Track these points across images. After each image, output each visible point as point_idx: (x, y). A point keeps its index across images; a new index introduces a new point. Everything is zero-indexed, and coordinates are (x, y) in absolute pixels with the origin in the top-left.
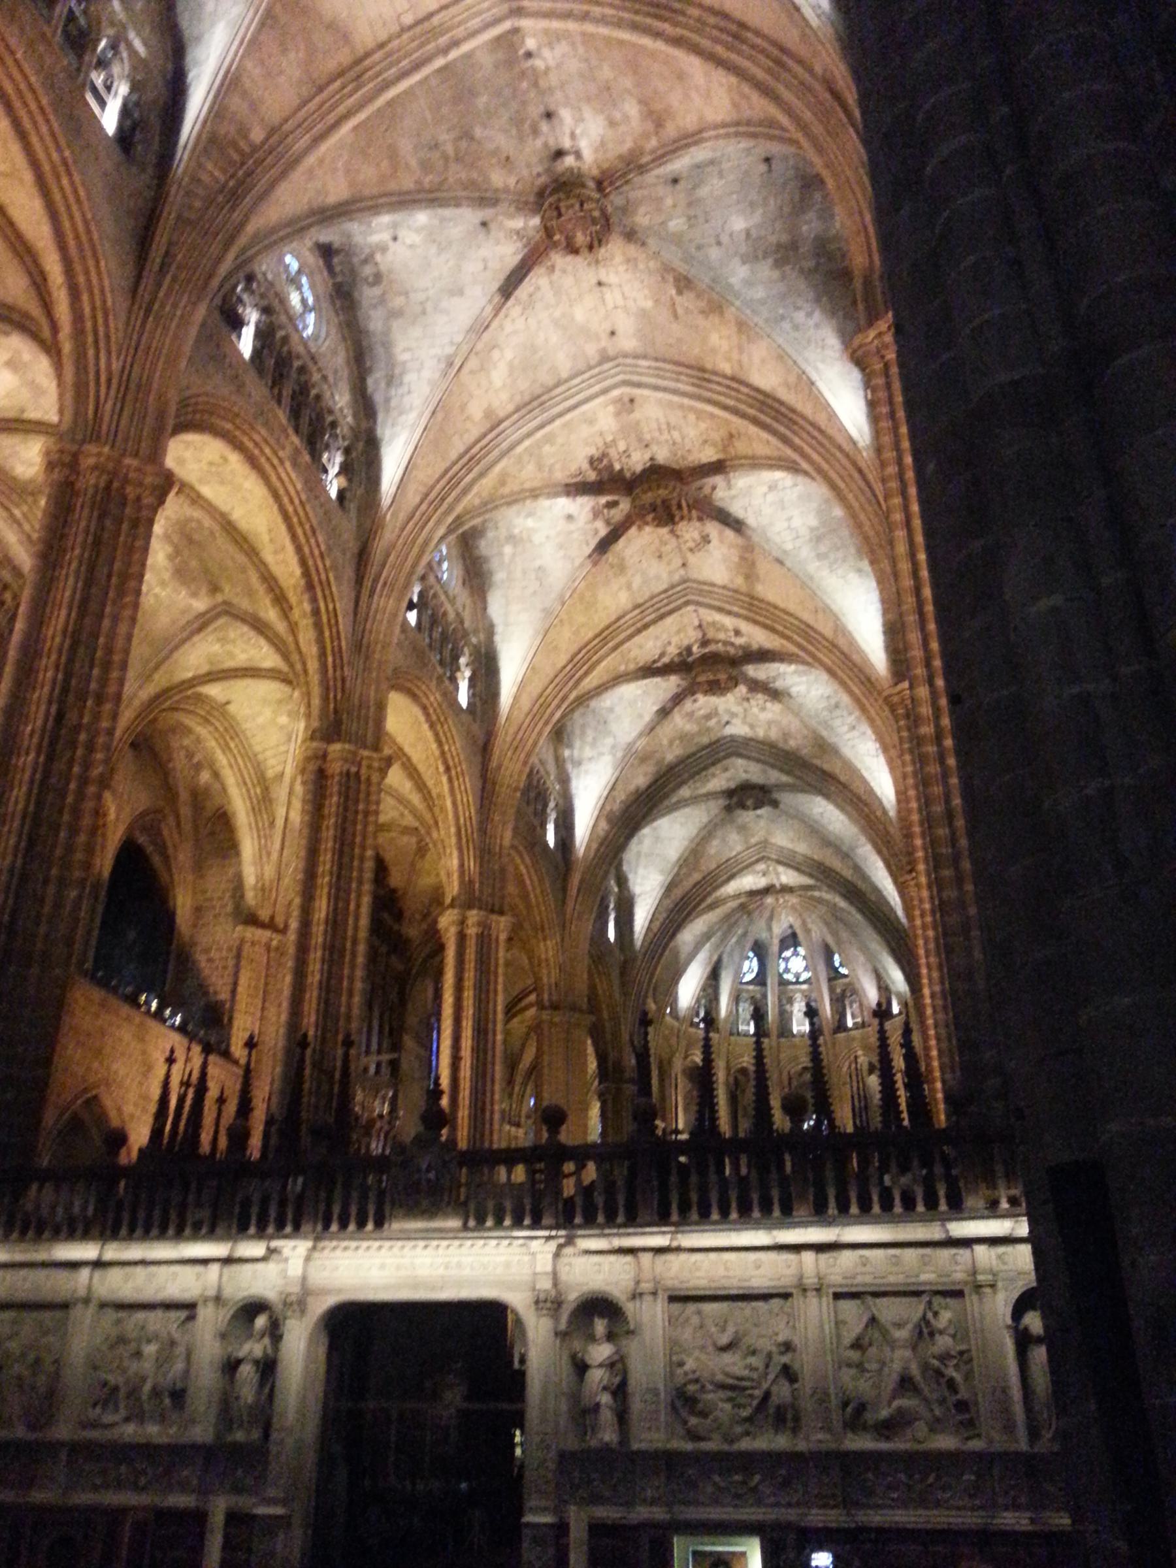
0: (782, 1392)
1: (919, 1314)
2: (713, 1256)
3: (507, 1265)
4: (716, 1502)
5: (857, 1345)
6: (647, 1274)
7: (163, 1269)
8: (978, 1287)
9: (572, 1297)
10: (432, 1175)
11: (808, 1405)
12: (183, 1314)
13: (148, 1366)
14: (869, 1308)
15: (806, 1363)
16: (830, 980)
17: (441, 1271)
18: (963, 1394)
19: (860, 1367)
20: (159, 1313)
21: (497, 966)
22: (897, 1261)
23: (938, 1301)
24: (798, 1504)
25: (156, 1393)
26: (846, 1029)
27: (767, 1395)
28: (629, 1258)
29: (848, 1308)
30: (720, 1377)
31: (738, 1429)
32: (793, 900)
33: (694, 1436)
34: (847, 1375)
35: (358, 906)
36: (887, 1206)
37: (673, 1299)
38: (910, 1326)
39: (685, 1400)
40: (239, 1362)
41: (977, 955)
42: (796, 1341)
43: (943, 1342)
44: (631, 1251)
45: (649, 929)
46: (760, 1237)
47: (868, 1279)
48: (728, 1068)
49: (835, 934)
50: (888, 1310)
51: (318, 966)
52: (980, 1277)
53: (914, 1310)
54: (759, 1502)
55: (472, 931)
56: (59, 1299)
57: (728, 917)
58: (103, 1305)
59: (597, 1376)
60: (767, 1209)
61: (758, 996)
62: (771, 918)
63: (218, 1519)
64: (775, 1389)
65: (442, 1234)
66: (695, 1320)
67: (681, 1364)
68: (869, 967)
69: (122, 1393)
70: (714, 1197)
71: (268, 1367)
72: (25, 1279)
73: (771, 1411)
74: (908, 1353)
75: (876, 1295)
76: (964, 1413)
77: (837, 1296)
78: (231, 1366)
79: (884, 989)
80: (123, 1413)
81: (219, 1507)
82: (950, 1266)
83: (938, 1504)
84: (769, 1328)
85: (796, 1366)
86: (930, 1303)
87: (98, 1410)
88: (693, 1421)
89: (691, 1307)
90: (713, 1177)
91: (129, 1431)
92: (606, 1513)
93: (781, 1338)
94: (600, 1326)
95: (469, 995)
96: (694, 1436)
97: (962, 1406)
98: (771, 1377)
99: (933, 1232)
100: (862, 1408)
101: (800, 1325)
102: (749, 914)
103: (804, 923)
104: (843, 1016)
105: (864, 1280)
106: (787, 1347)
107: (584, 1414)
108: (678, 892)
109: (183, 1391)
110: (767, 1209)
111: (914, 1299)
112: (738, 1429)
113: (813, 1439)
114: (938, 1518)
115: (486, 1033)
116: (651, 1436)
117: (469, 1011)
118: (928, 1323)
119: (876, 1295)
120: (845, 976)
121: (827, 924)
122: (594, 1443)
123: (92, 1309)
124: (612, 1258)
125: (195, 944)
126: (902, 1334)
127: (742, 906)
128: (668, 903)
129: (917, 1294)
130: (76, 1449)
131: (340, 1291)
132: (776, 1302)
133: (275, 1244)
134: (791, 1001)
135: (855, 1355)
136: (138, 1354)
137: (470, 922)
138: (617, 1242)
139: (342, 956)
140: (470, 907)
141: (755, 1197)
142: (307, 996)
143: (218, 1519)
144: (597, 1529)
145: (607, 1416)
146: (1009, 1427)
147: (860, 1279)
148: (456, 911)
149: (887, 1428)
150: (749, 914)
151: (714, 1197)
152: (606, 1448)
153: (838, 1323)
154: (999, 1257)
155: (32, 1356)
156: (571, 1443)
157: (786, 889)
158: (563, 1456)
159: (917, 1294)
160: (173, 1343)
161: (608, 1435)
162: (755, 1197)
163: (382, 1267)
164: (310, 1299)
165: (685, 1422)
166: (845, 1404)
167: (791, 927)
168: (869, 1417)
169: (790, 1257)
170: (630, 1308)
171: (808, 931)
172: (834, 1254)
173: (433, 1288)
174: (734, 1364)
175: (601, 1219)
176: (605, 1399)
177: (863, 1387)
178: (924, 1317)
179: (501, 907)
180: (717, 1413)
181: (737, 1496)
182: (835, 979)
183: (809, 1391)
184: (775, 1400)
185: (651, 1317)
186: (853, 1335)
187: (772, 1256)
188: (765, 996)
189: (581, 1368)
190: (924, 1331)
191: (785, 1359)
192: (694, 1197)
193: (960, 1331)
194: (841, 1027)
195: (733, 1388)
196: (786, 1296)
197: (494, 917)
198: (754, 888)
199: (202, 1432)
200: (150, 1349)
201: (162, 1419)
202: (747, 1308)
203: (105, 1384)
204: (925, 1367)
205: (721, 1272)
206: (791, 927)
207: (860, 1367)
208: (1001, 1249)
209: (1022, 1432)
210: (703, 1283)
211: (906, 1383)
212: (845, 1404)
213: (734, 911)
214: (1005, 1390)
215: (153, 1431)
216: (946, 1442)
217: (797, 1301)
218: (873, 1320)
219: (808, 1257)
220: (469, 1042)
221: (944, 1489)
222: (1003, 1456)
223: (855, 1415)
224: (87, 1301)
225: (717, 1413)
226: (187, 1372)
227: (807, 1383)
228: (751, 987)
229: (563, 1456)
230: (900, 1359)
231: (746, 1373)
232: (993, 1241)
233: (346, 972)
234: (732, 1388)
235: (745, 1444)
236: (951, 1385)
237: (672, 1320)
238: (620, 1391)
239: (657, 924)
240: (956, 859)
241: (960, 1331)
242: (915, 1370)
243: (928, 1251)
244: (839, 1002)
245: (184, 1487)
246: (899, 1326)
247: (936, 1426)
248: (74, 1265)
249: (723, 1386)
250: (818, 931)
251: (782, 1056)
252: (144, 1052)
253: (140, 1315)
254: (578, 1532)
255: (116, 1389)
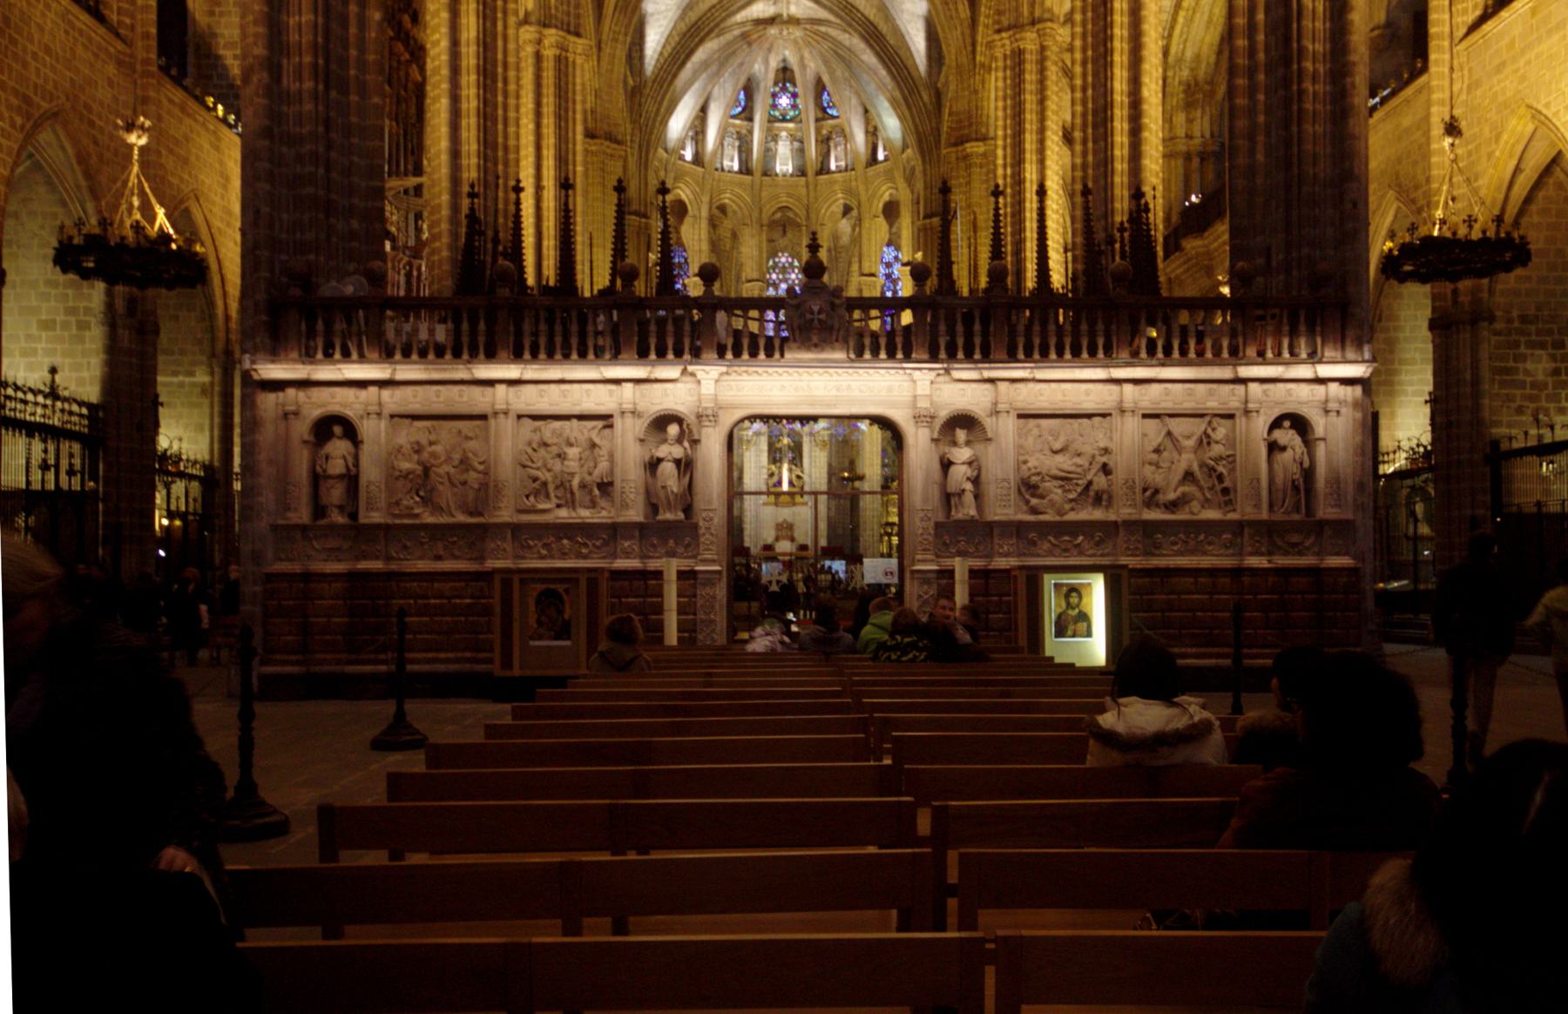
0: (1101, 482)
1: (1203, 428)
2: (1053, 385)
3: (890, 389)
4: (1050, 554)
5: (1157, 451)
6: (1003, 398)
7: (576, 386)
8: (1247, 412)
9: (944, 414)
10: (822, 317)
11: (1119, 491)
12: (600, 424)
13: (572, 465)
14: (1165, 425)
15: (1120, 463)
16: (817, 120)
17: (834, 392)
18: (1227, 484)
19: (1157, 466)
20: (575, 421)
21: (574, 93)
22: (1190, 393)
23: (1216, 421)
24: (1108, 555)
25: (583, 486)
26: (829, 172)
27: (1090, 483)
28: (988, 386)
29: (1152, 424)
30: (1055, 472)
31: (1067, 507)
32: (797, 33)
33: (1034, 511)
34: (1149, 470)
35: (505, 27)
36: (1151, 351)
37: (1020, 416)
38: (1195, 438)
39: (1028, 487)
40: (660, 460)
41: (1260, 157)
42: (1111, 446)
43: (1217, 450)
44: (992, 381)
45: (661, 54)
46: (1099, 373)
47: (1170, 405)
48: (711, 202)
49: (831, 73)
50: (1178, 426)
51: (473, 91)
52: (1251, 406)
53: (1199, 426)
54: (1081, 553)
55: (549, 53)
56: (477, 411)
57: (729, 44)
58: (519, 417)
59: (960, 473)
60: (1093, 353)
61: (744, 132)
62: (770, 50)
63: (671, 576)
64: (1096, 479)
65: (836, 364)
66: (1036, 432)
67: (1025, 462)
68: (860, 110)
69: (551, 487)
70: (1053, 341)
71: (685, 465)
72: (1087, 394)
73: (1092, 493)
74: (1192, 456)
75: (1171, 416)
76: (1227, 495)
77: (1145, 416)
78: (653, 465)
79: (873, 132)
80: (555, 501)
81: (671, 567)
82: (1230, 397)
83: (1205, 553)
84: (1093, 437)
85: (1111, 464)
86: (1210, 423)
87: (532, 498)
88: (1034, 501)
89: (1032, 422)
90: (1052, 327)
91: (563, 514)
92: (978, 563)
93: (1102, 445)
94: (961, 435)
95: (549, 122)
96: (1034, 511)
97: (1226, 491)
98: (1093, 471)
99: (1226, 373)
100: (1157, 492)
101: (1116, 436)
102: (750, 44)
103: (802, 58)
104: (826, 156)
105: (1167, 405)
106: (1106, 451)
107: (949, 498)
108: (693, 16)
109: (611, 484)
110: (1093, 353)
111: (1197, 420)
112: (1067, 507)
113: (1122, 512)
114: (1206, 562)
115: (567, 164)
116: (1003, 509)
117: (549, 141)
118: (1208, 436)
119: (1171, 416)
120: (833, 117)
121: (826, 62)
122: (960, 516)
123: (512, 416)
124: (974, 385)
125: (214, 35)
126: (1191, 443)
127: (744, 36)
128: (683, 27)
129: (1202, 416)
130: (516, 529)
131: (747, 406)
132: (1097, 419)
133: (690, 368)
134: (775, 139)
135: (1155, 456)
136: (561, 456)
137: (546, 42)
138: (987, 374)
139: (495, 81)
140: (545, 26)
141: (1085, 343)
142: (464, 123)
143: (671, 576)
144: (973, 573)
145: (969, 498)
146: (1257, 506)
147: (1163, 405)
148: (532, 29)
149: (1173, 506)
150: (750, 44)
151: (1053, 341)
152: (972, 521)
153: (1145, 435)
154: (1265, 392)
155: (457, 456)
156: (941, 518)
157: (794, 21)
158: (938, 525)
159: (1202, 416)
160: (593, 445)
161: (968, 509)
162: (1085, 343)
163: (783, 387)
164: (721, 413)
165: (1027, 502)
166: (1145, 490)
167: (784, 60)
168: (1161, 498)
169: (1114, 388)
170: (988, 423)
171: (803, 66)
172: (1146, 386)
173: (828, 405)
174: (1064, 462)
175: (977, 356)
176: (969, 486)
177: (1156, 478)
178: (1205, 432)
179: (578, 26)
180: (1052, 496)
181: (1066, 550)
182: (823, 119)
183: (1121, 482)
184: (1095, 487)
185: (1006, 428)
186: (1155, 444)
187: (1100, 386)
188: (751, 132)
189: (946, 465)
190: (1205, 440)
191: (1104, 459)
192: (1037, 341)
193: (1231, 441)
194: (823, 169)
195: (1065, 479)
196: (1104, 415)
197: (572, 38)
198: (761, 16)
199: (635, 514)
200: (573, 452)
201: (593, 504)
202: (1075, 423)
203: (535, 480)
204: (1202, 465)
205: (1060, 397)
206: (784, 60)
207: (1157, 466)
208: (1266, 386)
209: (1265, 506)
210: (1045, 405)
211: (1188, 476)
212: (1145, 490)
213: (736, 38)
214: (1258, 480)
215: (585, 514)
216: (1212, 514)
217: (1116, 419)
218: (1169, 434)
219: (1128, 388)
220: (552, 173)
221: (1210, 543)
222: (1251, 523)
223: (1151, 496)
224: (506, 413)
225: (1052, 496)
226: (611, 472)
227: (1120, 475)
228: (737, 122)
229: (938, 525)
230: (1187, 460)
231: (1073, 469)
232: (1136, 382)
233: (500, 99)
234: (1062, 479)
235: (1071, 516)
236: (1220, 478)
237: (1021, 434)
238: (976, 481)
239: (669, 49)
240: (1251, 72)
241: (1231, 441)
242: (1196, 468)
243: (1214, 386)
244: (825, 142)
245: (627, 555)
246: (1188, 437)
247: (1206, 503)
248: (491, 383)
249: (1056, 478)
250: (813, 65)
251: (764, 194)
252: (221, 163)
253: (557, 424)
254: (961, 575)
255: (545, 484)
